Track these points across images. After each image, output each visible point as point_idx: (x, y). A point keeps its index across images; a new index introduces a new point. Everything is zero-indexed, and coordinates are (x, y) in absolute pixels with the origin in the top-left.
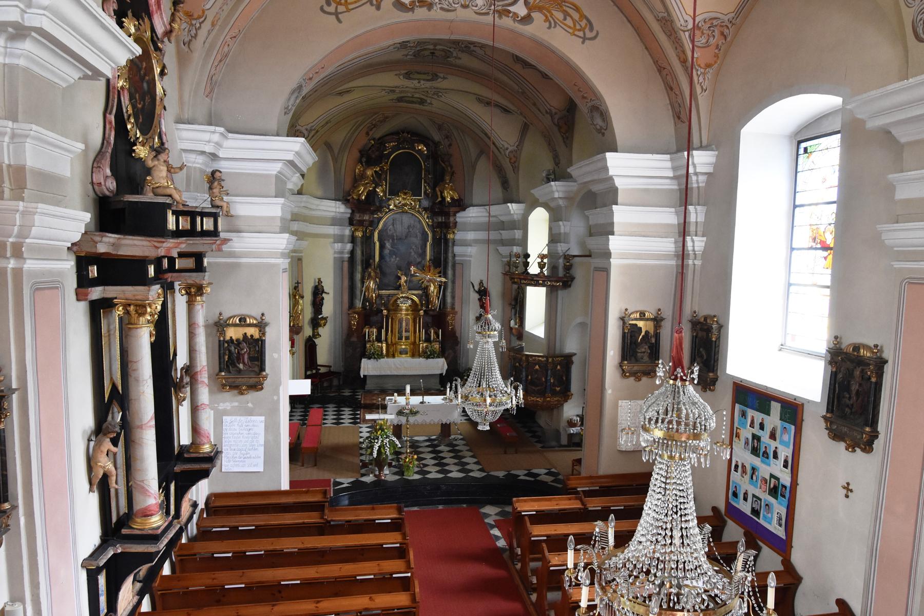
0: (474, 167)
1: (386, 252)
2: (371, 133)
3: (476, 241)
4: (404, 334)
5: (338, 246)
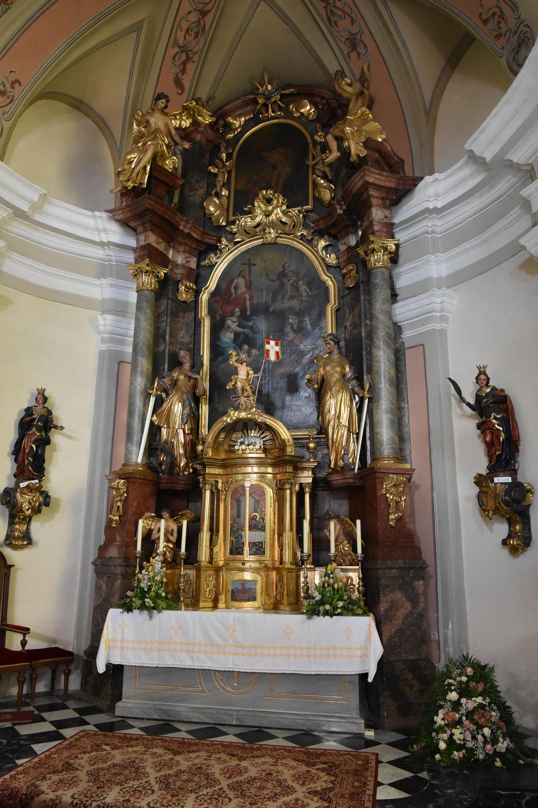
0: (430, 114)
1: (227, 337)
2: (186, 81)
3: (455, 280)
4: (248, 536)
5: (106, 321)
